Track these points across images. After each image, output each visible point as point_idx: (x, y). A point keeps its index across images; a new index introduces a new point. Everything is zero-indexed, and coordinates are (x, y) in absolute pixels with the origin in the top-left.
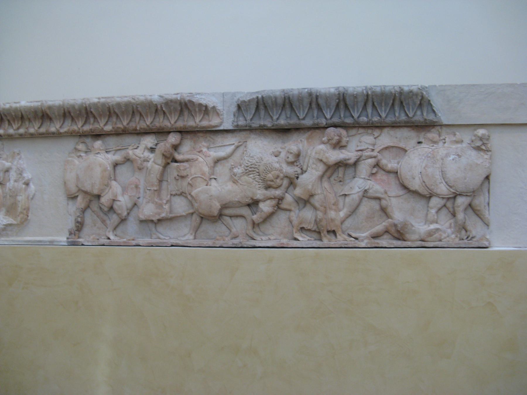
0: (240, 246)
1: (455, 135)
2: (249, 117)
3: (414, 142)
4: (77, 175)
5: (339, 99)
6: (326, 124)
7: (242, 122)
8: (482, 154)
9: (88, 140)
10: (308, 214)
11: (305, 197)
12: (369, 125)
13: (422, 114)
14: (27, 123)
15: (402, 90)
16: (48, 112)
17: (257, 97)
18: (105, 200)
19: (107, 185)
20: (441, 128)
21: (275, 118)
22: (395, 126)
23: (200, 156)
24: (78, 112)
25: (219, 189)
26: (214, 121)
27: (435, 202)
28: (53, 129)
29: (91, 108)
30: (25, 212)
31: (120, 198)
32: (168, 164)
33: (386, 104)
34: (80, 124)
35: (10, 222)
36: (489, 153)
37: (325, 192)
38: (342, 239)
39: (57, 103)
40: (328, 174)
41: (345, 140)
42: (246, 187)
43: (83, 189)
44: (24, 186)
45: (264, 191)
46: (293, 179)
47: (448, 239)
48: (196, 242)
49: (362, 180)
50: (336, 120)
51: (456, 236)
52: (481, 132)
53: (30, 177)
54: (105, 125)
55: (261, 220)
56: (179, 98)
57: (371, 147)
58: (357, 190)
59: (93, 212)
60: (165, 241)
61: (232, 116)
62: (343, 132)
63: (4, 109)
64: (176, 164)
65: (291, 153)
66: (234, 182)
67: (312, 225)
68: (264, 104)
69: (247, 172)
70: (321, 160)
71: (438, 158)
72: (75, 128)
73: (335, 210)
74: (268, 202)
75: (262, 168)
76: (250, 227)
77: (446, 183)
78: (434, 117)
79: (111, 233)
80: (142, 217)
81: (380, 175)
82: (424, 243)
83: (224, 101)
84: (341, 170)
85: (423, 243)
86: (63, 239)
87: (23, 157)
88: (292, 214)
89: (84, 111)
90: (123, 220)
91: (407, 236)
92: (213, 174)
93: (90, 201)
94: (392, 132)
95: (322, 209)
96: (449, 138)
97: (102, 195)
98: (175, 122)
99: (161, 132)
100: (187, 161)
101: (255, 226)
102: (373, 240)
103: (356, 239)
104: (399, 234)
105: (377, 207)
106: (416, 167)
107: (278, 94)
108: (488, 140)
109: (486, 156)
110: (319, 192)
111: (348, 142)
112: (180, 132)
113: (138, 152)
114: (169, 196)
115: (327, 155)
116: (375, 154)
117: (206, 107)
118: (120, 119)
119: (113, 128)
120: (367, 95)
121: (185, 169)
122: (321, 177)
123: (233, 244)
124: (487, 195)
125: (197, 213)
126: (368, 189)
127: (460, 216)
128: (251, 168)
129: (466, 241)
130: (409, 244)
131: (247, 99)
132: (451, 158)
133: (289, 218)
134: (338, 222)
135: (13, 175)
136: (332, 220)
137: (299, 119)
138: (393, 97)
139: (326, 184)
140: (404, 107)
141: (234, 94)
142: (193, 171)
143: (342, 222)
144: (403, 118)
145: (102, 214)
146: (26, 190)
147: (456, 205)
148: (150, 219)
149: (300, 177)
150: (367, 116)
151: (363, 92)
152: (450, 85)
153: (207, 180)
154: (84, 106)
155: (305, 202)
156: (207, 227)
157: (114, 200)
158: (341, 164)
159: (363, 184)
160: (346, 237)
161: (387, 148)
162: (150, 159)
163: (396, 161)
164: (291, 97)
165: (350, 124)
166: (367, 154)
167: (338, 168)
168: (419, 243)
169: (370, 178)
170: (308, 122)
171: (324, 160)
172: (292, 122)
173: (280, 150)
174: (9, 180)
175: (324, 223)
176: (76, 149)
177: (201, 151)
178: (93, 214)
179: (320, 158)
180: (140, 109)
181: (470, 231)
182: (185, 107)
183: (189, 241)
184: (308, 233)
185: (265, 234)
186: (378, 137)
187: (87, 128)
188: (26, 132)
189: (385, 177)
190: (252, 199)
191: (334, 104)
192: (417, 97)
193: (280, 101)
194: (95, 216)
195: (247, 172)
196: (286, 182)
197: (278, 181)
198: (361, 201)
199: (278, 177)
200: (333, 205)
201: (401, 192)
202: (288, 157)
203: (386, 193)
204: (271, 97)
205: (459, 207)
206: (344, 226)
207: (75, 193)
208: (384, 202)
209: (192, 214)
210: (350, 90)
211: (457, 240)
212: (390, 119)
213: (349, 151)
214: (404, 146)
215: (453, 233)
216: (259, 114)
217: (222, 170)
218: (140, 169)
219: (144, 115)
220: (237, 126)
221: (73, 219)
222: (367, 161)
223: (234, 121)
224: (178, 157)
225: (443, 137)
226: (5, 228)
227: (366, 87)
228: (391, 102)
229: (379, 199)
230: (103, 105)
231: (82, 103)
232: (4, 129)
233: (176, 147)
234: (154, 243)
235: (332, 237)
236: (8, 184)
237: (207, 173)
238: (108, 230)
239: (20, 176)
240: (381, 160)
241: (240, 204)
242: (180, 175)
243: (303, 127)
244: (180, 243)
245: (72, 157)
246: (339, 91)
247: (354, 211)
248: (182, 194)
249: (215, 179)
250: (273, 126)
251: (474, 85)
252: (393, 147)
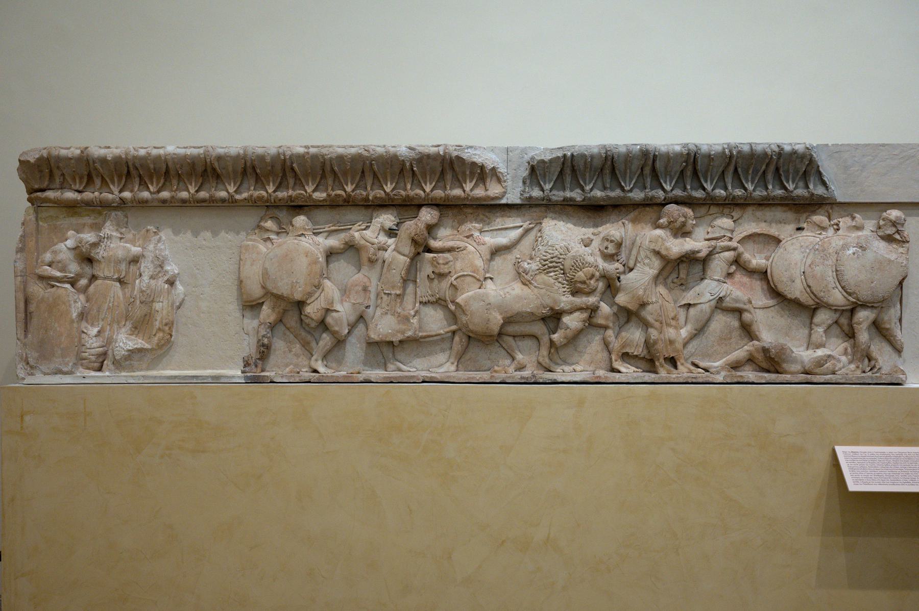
0: (533, 381)
1: (853, 218)
2: (547, 187)
3: (791, 228)
4: (266, 269)
5: (686, 162)
6: (665, 198)
7: (536, 193)
8: (895, 246)
9: (283, 215)
10: (635, 336)
11: (632, 307)
13: (807, 187)
14: (175, 182)
15: (782, 149)
16: (216, 165)
17: (565, 156)
18: (312, 310)
19: (318, 286)
20: (831, 208)
21: (588, 188)
22: (765, 203)
23: (470, 244)
24: (269, 168)
25: (497, 293)
26: (494, 190)
27: (823, 317)
28: (223, 194)
29: (292, 163)
30: (167, 328)
31: (338, 307)
32: (419, 253)
33: (756, 172)
34: (271, 189)
35: (139, 346)
36: (907, 245)
37: (662, 299)
38: (685, 370)
39: (233, 151)
40: (665, 273)
42: (544, 290)
43: (275, 291)
44: (166, 286)
45: (571, 298)
46: (613, 279)
47: (843, 370)
48: (463, 375)
49: (715, 283)
50: (678, 192)
51: (858, 367)
52: (894, 214)
53: (176, 272)
54: (314, 191)
55: (565, 341)
56: (441, 153)
58: (708, 297)
59: (288, 329)
60: (412, 374)
61: (521, 184)
62: (689, 211)
63: (135, 157)
64: (432, 255)
65: (612, 241)
66: (524, 284)
67: (641, 350)
68: (573, 166)
69: (546, 269)
70: (657, 253)
71: (831, 251)
72: (264, 193)
73: (676, 328)
74: (577, 314)
75: (568, 263)
76: (544, 352)
77: (843, 288)
78: (825, 192)
79: (320, 362)
80: (374, 336)
82: (810, 375)
83: (508, 161)
85: (809, 376)
86: (235, 372)
87: (164, 238)
88: (610, 333)
89: (278, 168)
90: (339, 342)
91: (785, 366)
92: (488, 272)
93: (285, 311)
94: (759, 214)
95: (657, 324)
96: (845, 222)
97: (308, 302)
98: (432, 191)
99: (406, 205)
100: (450, 250)
101: (552, 351)
102: (734, 372)
103: (706, 370)
104: (771, 363)
105: (736, 324)
106: (796, 264)
107: (596, 151)
108: (903, 225)
109: (901, 250)
110: (654, 300)
112: (437, 205)
113: (368, 234)
114: (417, 305)
115: (668, 244)
116: (734, 244)
117: (482, 167)
118: (340, 182)
119: (329, 195)
120: (731, 156)
121: (447, 263)
122: (656, 279)
123: (522, 378)
124: (899, 306)
125: (464, 330)
127: (863, 336)
128: (551, 262)
129: (870, 374)
130: (788, 377)
131: (547, 157)
132: (851, 252)
133: (604, 339)
134: (679, 346)
135: (146, 267)
136: (671, 342)
137: (623, 190)
138: (767, 161)
139: (661, 289)
140: (780, 175)
141: (524, 150)
142: (459, 266)
143: (685, 345)
144: (779, 192)
145: (303, 334)
146: (169, 292)
147: (855, 320)
148: (388, 339)
149: (622, 277)
150: (726, 189)
151: (724, 152)
152: (848, 145)
153: (482, 279)
154: (282, 157)
155: (629, 315)
156: (478, 353)
157: (328, 311)
158: (684, 259)
160: (692, 368)
161: (751, 237)
162: (389, 246)
163: (763, 256)
164: (616, 156)
165: (701, 199)
166: (722, 244)
168: (802, 377)
170: (638, 195)
171: (664, 252)
172: (612, 194)
173: (592, 237)
174: (141, 275)
175: (660, 346)
176: (259, 227)
177: (472, 235)
178: (288, 333)
179: (657, 249)
180: (375, 167)
181: (876, 360)
182: (450, 166)
183: (448, 374)
184: (632, 361)
185: (565, 362)
187: (281, 194)
188: (173, 197)
189: (746, 279)
190: (552, 309)
191: (677, 168)
192: (802, 161)
193: (597, 163)
194: (292, 336)
195: (546, 269)
196: (601, 285)
197: (592, 282)
198: (712, 313)
199: (593, 276)
201: (771, 302)
202: (607, 248)
203: (750, 302)
204: (585, 155)
205: (859, 324)
206: (685, 352)
207: (260, 299)
208: (746, 316)
209: (454, 332)
210: (704, 149)
211: (859, 372)
212: (759, 193)
214: (776, 234)
215: (850, 362)
216: (563, 182)
217: (504, 264)
218: (372, 262)
219: (380, 177)
220: (531, 198)
221: (255, 340)
223: (524, 191)
224: (434, 244)
225: (835, 221)
226: (129, 355)
227: (728, 144)
228: (764, 167)
229: (739, 312)
230: (315, 157)
231: (279, 154)
232: (132, 191)
233: (431, 229)
234: (396, 378)
235: (668, 367)
236: (137, 281)
237: (481, 269)
238: (314, 358)
239: (159, 269)
240: (743, 253)
241: (531, 318)
242: (437, 271)
243: (629, 202)
244: (438, 377)
245: (254, 240)
246: (689, 150)
247: (699, 332)
248: (439, 302)
249: (491, 279)
250: (584, 200)
251: (883, 145)
252: (759, 235)
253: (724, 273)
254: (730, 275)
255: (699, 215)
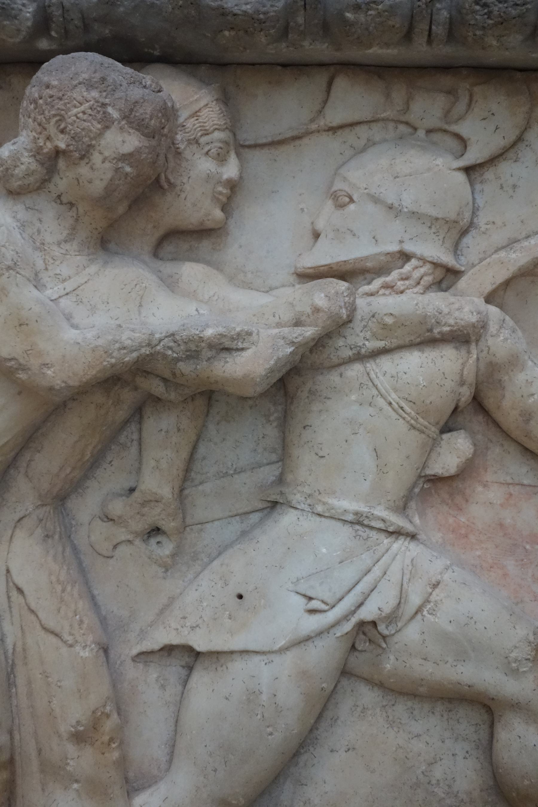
12: (420, 51)
41: (202, 171)
57: (434, 250)
58: (289, 617)
62: (193, 102)
81: (495, 494)
84: (162, 441)
111: (231, 195)
126: (392, 618)
158: (157, 388)
159: (349, 574)
166: (388, 305)
167: (138, 413)
169: (415, 522)
186: (493, 160)
198: (320, 712)
200: (78, 738)
213: (239, 280)
222: (386, 364)
240: (514, 362)
253: (396, 482)
254: (432, 487)
255: (266, 131)
